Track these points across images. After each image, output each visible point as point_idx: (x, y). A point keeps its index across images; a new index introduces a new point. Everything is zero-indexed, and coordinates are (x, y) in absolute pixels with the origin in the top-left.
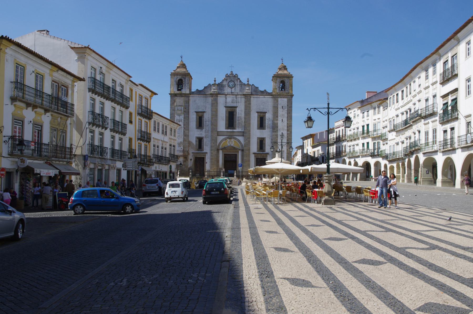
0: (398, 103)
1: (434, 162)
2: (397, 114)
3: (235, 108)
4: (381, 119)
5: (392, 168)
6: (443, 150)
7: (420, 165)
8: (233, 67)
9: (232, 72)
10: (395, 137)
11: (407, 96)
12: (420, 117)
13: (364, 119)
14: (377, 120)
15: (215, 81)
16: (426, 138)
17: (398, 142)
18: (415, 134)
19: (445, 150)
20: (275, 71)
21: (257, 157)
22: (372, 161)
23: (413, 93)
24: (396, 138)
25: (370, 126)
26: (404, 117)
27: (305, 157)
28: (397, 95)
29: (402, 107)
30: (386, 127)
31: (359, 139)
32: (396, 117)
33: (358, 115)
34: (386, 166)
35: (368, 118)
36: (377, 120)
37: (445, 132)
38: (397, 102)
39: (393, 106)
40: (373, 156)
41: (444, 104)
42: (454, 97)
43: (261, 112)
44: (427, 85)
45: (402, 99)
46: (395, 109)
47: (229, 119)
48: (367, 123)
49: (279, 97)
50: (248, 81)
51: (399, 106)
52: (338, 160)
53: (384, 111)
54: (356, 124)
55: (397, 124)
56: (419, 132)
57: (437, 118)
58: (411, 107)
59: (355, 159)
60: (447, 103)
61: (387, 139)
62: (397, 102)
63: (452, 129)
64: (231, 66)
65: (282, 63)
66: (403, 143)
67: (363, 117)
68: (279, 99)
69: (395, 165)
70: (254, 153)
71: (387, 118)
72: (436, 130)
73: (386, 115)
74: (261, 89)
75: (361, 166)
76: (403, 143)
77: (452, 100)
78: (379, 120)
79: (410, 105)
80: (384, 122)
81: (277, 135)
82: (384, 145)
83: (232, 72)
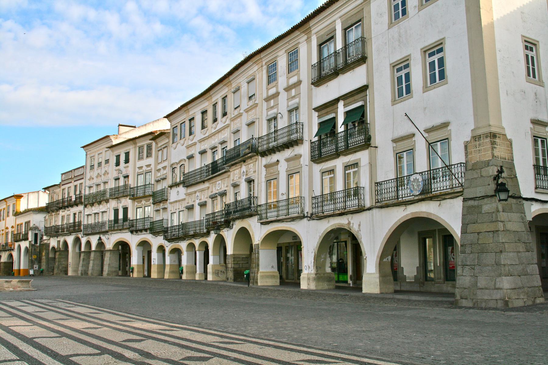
2: (190, 153)
5: (177, 252)
11: (215, 120)
13: (118, 167)
17: (193, 205)
18: (236, 186)
22: (133, 240)
24: (187, 197)
26: (208, 160)
27: (3, 234)
30: (164, 179)
31: (107, 201)
32: (187, 160)
33: (107, 161)
34: (161, 249)
35: (127, 165)
40: (134, 231)
44: (272, 91)
45: (203, 127)
46: (185, 145)
52: (65, 238)
53: (160, 152)
54: (102, 176)
56: (250, 181)
57: (304, 150)
59: (100, 238)
61: (167, 200)
66: (203, 205)
67: (118, 164)
69: (183, 245)
73: (165, 159)
75: (111, 249)
76: (203, 205)
78: (149, 168)
79: (225, 135)
80: (159, 170)
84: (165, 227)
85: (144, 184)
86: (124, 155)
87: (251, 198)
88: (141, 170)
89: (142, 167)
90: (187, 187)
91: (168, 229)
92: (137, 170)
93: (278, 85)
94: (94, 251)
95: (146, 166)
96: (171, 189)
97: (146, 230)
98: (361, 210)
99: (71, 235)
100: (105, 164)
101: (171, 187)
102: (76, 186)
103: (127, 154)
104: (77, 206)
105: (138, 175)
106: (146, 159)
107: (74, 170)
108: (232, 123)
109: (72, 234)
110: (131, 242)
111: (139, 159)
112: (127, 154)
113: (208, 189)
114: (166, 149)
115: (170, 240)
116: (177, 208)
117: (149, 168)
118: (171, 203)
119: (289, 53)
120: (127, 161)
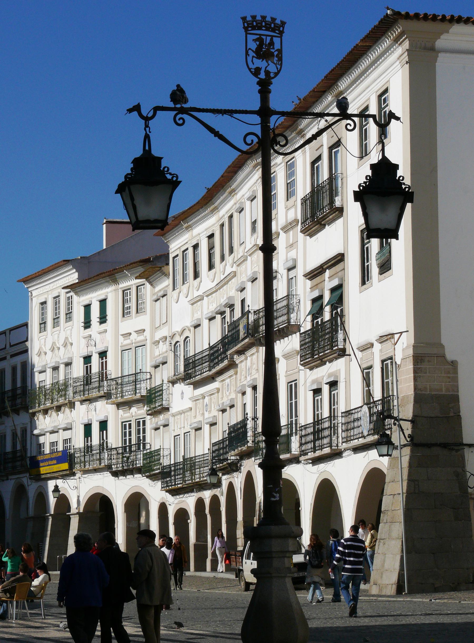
0: (198, 280)
1: (297, 497)
4: (147, 333)
6: (311, 455)
7: (257, 508)
10: (190, 404)
11: (223, 258)
12: (252, 340)
14: (134, 336)
16: (291, 404)
18: (244, 394)
19: (318, 453)
23: (239, 252)
25: (110, 355)
28: (196, 247)
29: (210, 293)
31: (72, 405)
32: (192, 329)
34: (163, 509)
36: (134, 336)
37: (317, 392)
38: (196, 275)
39: (184, 288)
41: (314, 301)
42: (335, 282)
45: (211, 266)
46: (189, 298)
48: (101, 348)
51: (200, 293)
53: (158, 302)
55: (195, 355)
58: (230, 298)
60: (320, 297)
61: (167, 409)
62: (196, 275)
63: (333, 384)
67: (87, 324)
71: (164, 332)
72: (296, 384)
77: (333, 290)
78: (141, 338)
82: (157, 429)
84: (165, 464)
85: (134, 372)
86: (98, 303)
87: (248, 419)
88: (128, 342)
89: (130, 334)
90: (196, 385)
91: (170, 468)
92: (121, 338)
93: (278, 218)
94: (32, 517)
95: (135, 332)
96: (173, 386)
97: (139, 471)
98: (337, 454)
99: (8, 479)
100: (54, 327)
101: (173, 383)
102: (14, 369)
103: (103, 303)
104: (18, 415)
105: (122, 351)
106: (135, 318)
107: (11, 330)
108: (239, 268)
109: (10, 477)
110: (114, 495)
111: (124, 316)
112: (103, 303)
113: (218, 392)
114: (165, 297)
115: (174, 492)
116: (182, 426)
117: (141, 338)
118: (174, 415)
119: (287, 162)
120: (103, 319)
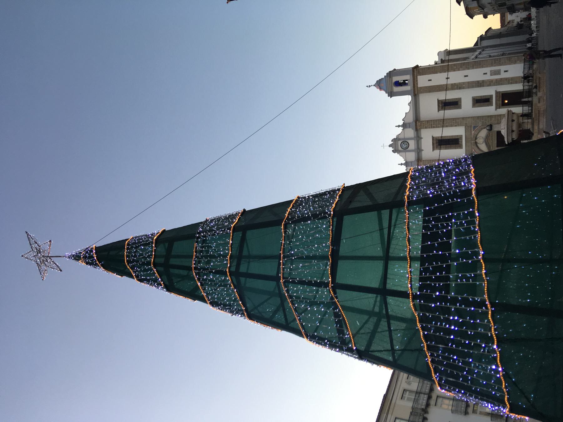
3: (434, 138)
8: (383, 144)
9: (390, 146)
15: (402, 164)
20: (383, 94)
21: (501, 105)
43: (439, 106)
47: (449, 144)
49: (417, 87)
50: (399, 126)
64: (383, 147)
65: (374, 85)
68: (419, 86)
70: (496, 109)
74: (407, 109)
81: (468, 82)
83: (390, 146)
